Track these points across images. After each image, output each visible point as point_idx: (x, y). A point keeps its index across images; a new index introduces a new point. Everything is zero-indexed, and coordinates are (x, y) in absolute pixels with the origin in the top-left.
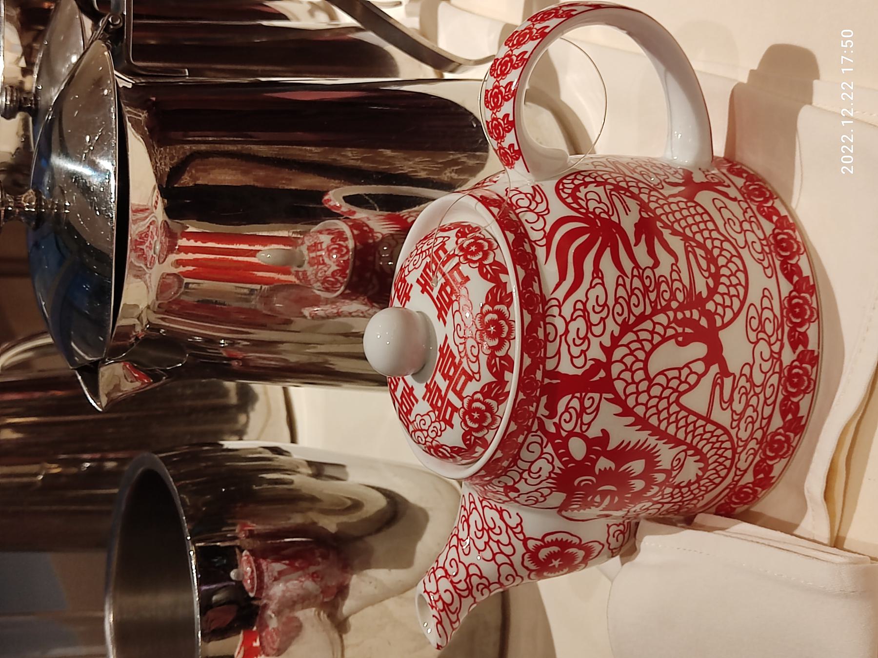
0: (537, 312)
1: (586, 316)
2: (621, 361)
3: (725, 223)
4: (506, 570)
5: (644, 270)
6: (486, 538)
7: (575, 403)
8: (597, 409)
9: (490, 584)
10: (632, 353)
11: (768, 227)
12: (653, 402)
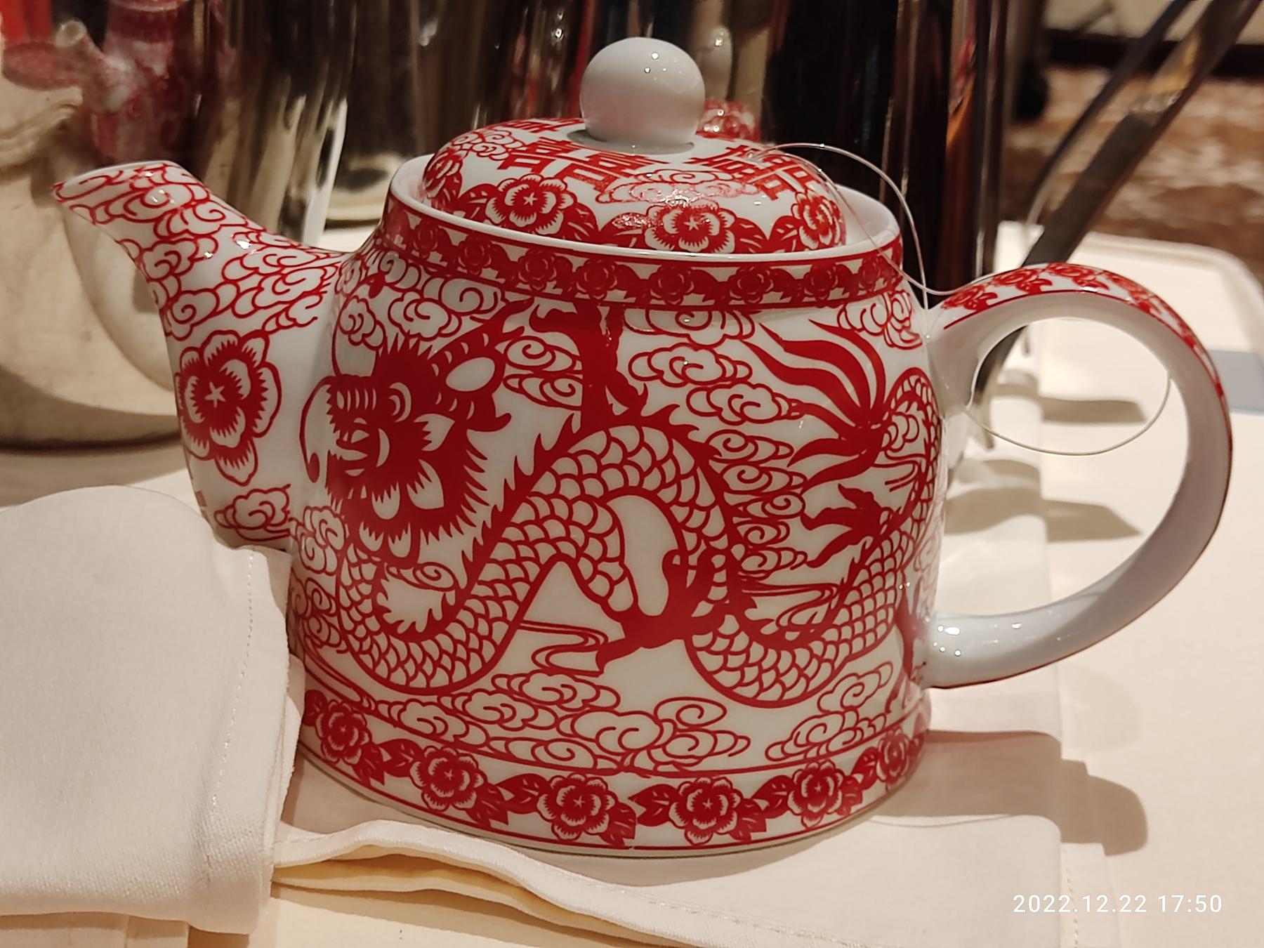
0: (732, 295)
1: (726, 381)
2: (642, 444)
3: (859, 677)
4: (205, 304)
5: (799, 496)
6: (265, 269)
7: (562, 362)
8: (551, 403)
9: (177, 276)
10: (657, 464)
11: (846, 762)
12: (561, 509)
